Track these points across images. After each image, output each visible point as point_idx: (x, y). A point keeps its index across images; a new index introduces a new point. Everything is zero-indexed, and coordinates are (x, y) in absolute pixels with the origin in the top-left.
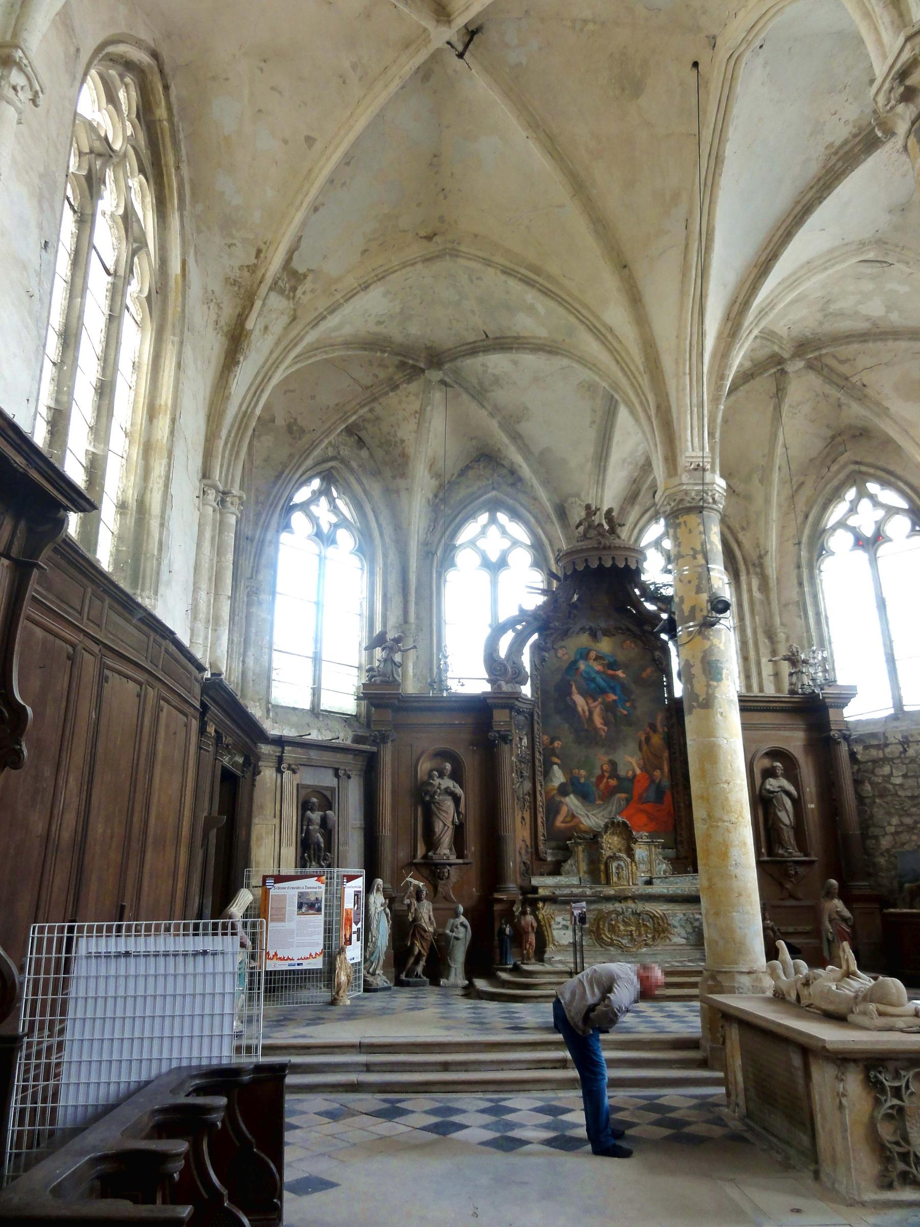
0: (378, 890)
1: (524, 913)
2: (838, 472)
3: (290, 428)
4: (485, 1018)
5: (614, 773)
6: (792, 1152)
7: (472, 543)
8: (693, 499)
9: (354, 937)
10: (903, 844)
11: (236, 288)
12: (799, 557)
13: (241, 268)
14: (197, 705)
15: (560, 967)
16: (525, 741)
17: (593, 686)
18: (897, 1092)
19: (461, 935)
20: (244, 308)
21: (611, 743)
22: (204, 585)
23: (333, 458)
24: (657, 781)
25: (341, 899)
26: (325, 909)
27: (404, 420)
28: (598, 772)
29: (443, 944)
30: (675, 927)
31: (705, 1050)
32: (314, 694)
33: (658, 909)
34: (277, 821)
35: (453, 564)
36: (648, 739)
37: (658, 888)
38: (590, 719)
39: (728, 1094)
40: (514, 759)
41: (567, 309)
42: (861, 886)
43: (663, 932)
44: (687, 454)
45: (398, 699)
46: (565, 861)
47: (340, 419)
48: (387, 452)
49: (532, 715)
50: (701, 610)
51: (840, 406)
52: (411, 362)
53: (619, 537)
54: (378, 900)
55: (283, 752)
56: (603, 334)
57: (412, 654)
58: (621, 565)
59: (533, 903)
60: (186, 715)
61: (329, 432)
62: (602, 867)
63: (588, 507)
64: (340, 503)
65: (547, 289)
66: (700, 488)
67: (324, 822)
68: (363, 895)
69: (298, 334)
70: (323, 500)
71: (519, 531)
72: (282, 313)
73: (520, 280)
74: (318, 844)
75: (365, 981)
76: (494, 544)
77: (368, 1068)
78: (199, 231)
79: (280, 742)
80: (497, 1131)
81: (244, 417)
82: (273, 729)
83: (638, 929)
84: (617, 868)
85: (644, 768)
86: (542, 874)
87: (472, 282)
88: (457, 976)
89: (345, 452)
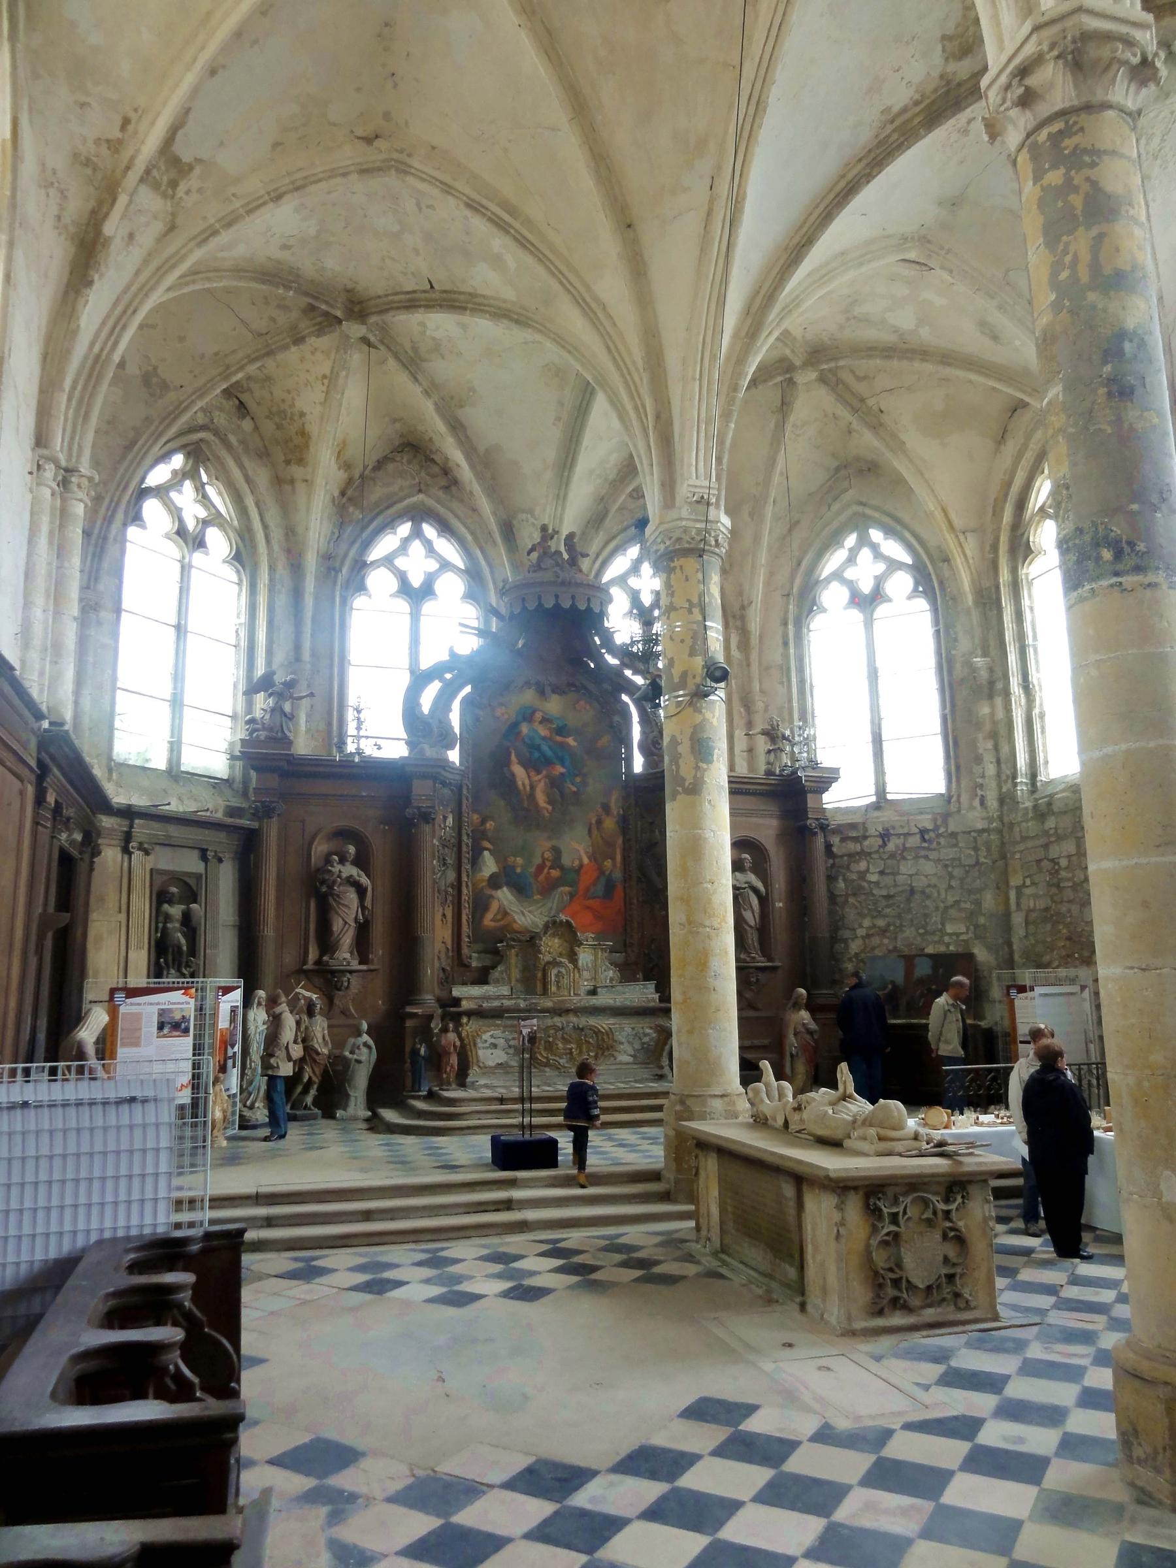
0: (259, 1004)
1: (445, 1030)
2: (839, 513)
3: (147, 379)
4: (404, 1156)
5: (557, 863)
6: (774, 1285)
8: (693, 539)
10: (873, 949)
11: (89, 171)
12: (786, 612)
13: (98, 141)
14: (33, 764)
15: (488, 1093)
16: (450, 821)
17: (536, 755)
18: (894, 1219)
19: (363, 1058)
20: (100, 203)
21: (555, 826)
22: (39, 600)
23: (203, 428)
24: (607, 873)
25: (215, 1015)
26: (195, 1029)
27: (306, 385)
28: (537, 861)
29: (340, 1068)
30: (621, 1043)
31: (668, 1183)
32: (171, 750)
33: (604, 1023)
34: (123, 917)
36: (599, 822)
37: (604, 999)
38: (532, 797)
39: (698, 1228)
40: (436, 842)
41: (547, 268)
42: (825, 994)
43: (608, 1049)
44: (691, 482)
45: (289, 762)
46: (494, 967)
47: (220, 375)
48: (279, 427)
49: (460, 788)
50: (694, 677)
51: (850, 432)
52: (324, 307)
53: (581, 571)
55: (131, 826)
56: (590, 308)
57: (305, 704)
58: (582, 606)
59: (456, 1018)
60: (22, 780)
61: (202, 392)
62: (540, 975)
63: (544, 528)
64: (210, 491)
65: (525, 238)
66: (702, 525)
67: (187, 918)
68: (240, 1011)
69: (177, 252)
70: (188, 485)
71: (447, 549)
72: (155, 218)
73: (490, 220)
74: (179, 947)
75: (241, 1116)
76: (416, 565)
78: (35, 76)
79: (128, 813)
80: (443, 1285)
81: (95, 365)
82: (119, 797)
83: (579, 1047)
84: (557, 976)
85: (593, 857)
86: (464, 984)
87: (420, 209)
88: (357, 1105)
89: (220, 419)
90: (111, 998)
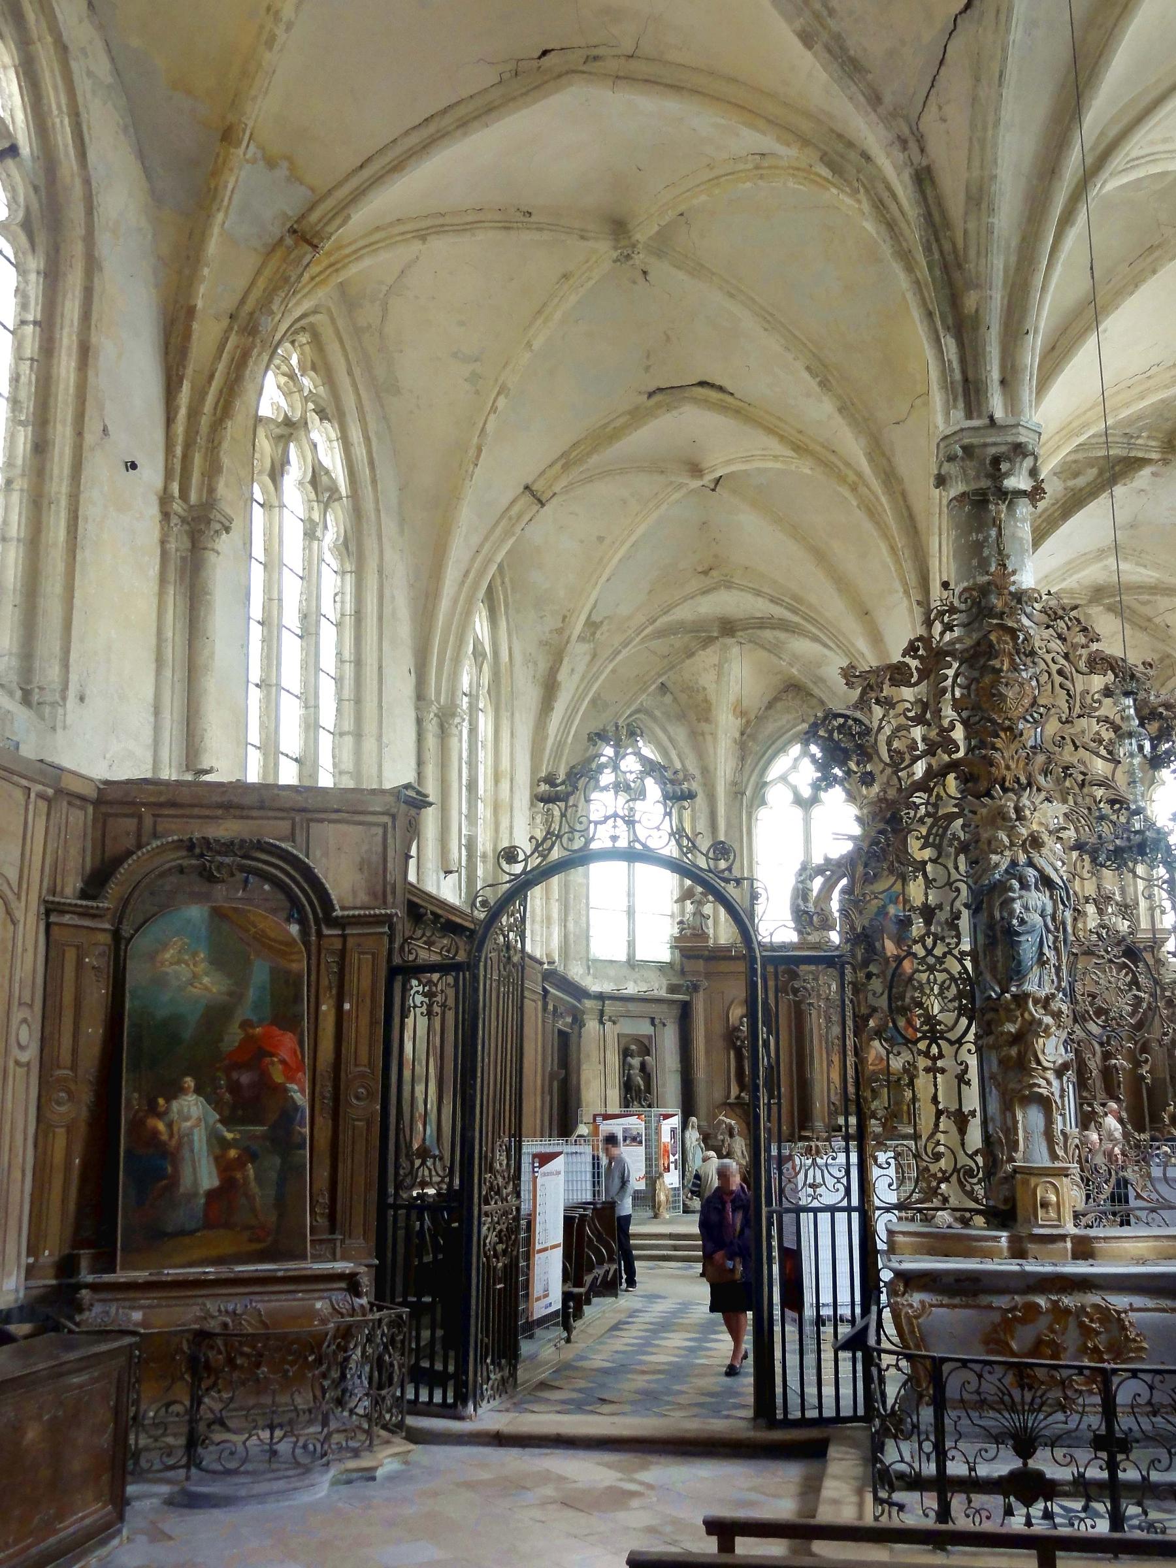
7: (783, 778)
9: (672, 1166)
13: (551, 632)
35: (763, 803)
48: (690, 697)
54: (693, 1136)
68: (679, 1131)
77: (675, 1248)
79: (601, 997)
82: (595, 986)
90: (595, 1120)
